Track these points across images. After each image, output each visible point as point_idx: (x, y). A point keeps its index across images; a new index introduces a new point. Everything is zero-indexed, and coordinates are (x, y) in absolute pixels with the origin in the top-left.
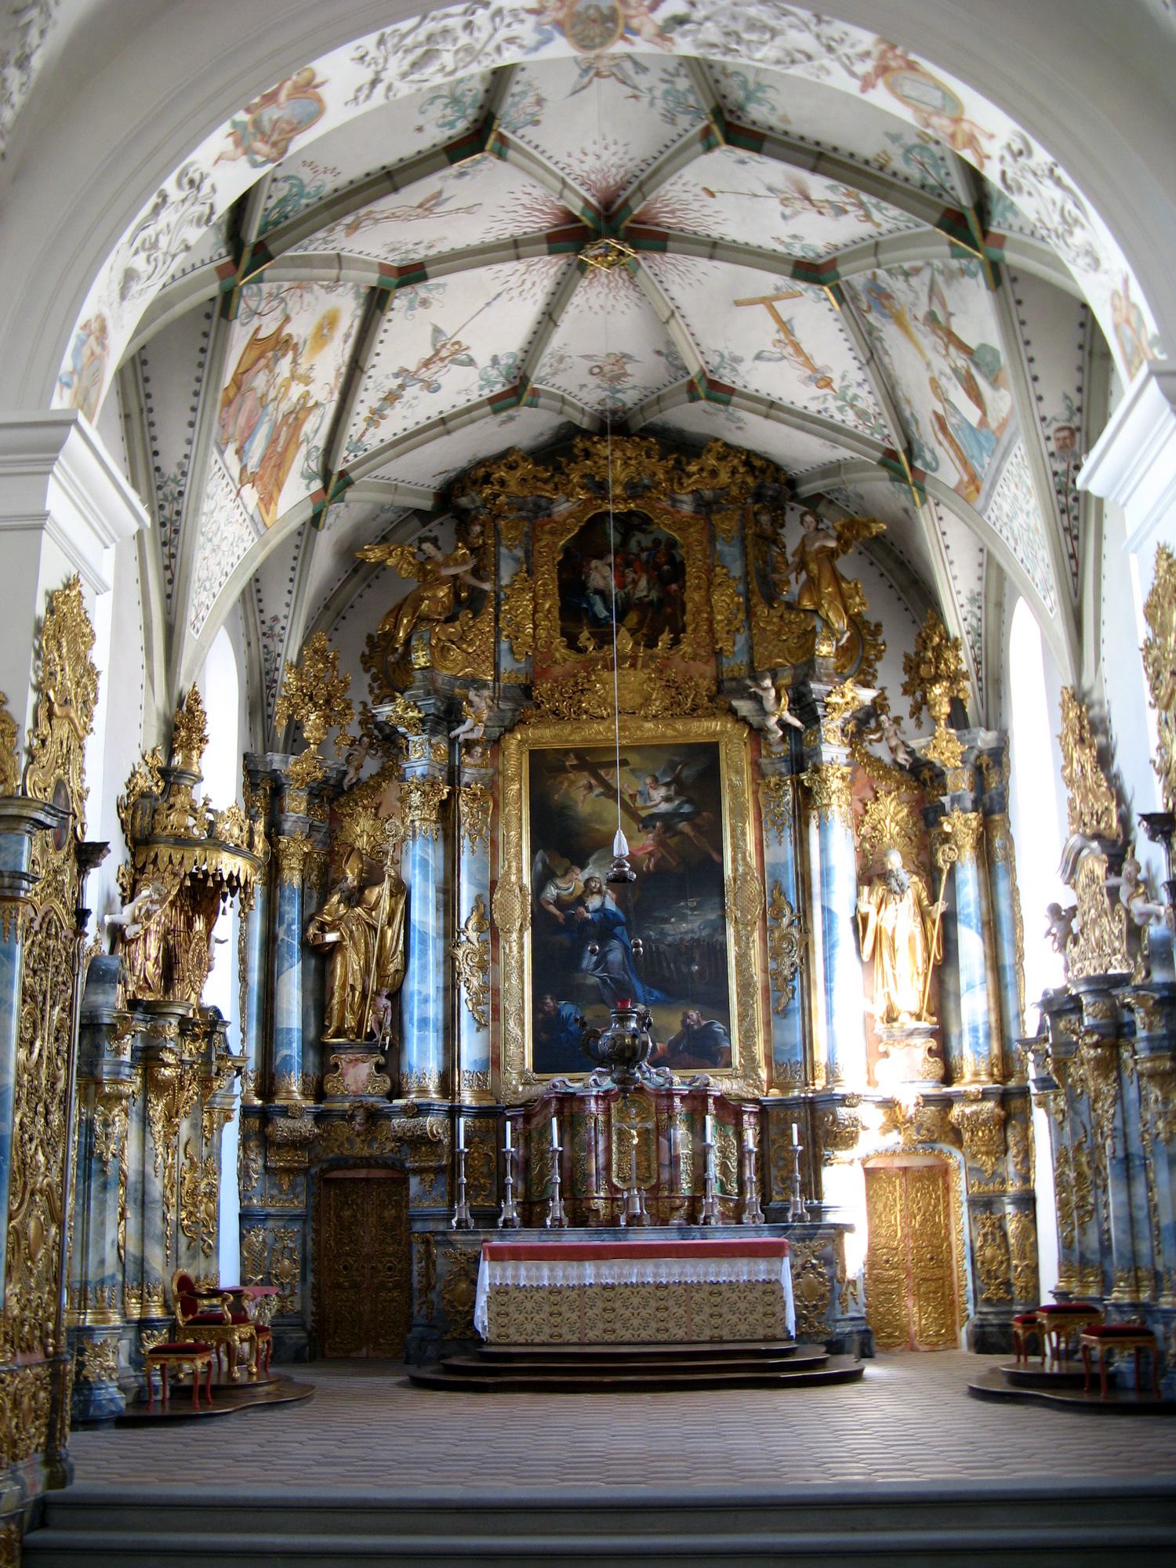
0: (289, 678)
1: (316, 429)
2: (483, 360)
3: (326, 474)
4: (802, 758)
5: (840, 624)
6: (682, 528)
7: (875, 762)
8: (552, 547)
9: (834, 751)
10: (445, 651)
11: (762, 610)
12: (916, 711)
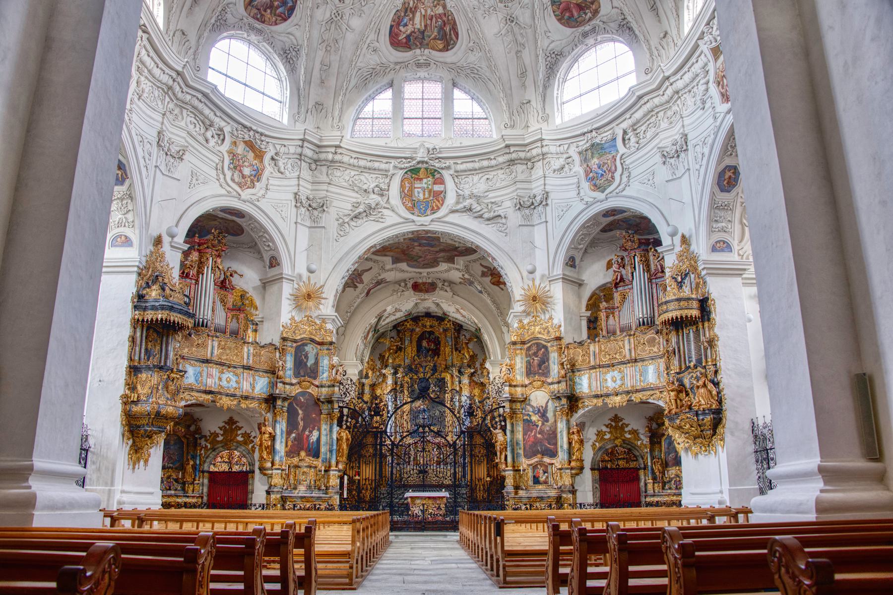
6: (440, 334)
7: (474, 381)
8: (415, 338)
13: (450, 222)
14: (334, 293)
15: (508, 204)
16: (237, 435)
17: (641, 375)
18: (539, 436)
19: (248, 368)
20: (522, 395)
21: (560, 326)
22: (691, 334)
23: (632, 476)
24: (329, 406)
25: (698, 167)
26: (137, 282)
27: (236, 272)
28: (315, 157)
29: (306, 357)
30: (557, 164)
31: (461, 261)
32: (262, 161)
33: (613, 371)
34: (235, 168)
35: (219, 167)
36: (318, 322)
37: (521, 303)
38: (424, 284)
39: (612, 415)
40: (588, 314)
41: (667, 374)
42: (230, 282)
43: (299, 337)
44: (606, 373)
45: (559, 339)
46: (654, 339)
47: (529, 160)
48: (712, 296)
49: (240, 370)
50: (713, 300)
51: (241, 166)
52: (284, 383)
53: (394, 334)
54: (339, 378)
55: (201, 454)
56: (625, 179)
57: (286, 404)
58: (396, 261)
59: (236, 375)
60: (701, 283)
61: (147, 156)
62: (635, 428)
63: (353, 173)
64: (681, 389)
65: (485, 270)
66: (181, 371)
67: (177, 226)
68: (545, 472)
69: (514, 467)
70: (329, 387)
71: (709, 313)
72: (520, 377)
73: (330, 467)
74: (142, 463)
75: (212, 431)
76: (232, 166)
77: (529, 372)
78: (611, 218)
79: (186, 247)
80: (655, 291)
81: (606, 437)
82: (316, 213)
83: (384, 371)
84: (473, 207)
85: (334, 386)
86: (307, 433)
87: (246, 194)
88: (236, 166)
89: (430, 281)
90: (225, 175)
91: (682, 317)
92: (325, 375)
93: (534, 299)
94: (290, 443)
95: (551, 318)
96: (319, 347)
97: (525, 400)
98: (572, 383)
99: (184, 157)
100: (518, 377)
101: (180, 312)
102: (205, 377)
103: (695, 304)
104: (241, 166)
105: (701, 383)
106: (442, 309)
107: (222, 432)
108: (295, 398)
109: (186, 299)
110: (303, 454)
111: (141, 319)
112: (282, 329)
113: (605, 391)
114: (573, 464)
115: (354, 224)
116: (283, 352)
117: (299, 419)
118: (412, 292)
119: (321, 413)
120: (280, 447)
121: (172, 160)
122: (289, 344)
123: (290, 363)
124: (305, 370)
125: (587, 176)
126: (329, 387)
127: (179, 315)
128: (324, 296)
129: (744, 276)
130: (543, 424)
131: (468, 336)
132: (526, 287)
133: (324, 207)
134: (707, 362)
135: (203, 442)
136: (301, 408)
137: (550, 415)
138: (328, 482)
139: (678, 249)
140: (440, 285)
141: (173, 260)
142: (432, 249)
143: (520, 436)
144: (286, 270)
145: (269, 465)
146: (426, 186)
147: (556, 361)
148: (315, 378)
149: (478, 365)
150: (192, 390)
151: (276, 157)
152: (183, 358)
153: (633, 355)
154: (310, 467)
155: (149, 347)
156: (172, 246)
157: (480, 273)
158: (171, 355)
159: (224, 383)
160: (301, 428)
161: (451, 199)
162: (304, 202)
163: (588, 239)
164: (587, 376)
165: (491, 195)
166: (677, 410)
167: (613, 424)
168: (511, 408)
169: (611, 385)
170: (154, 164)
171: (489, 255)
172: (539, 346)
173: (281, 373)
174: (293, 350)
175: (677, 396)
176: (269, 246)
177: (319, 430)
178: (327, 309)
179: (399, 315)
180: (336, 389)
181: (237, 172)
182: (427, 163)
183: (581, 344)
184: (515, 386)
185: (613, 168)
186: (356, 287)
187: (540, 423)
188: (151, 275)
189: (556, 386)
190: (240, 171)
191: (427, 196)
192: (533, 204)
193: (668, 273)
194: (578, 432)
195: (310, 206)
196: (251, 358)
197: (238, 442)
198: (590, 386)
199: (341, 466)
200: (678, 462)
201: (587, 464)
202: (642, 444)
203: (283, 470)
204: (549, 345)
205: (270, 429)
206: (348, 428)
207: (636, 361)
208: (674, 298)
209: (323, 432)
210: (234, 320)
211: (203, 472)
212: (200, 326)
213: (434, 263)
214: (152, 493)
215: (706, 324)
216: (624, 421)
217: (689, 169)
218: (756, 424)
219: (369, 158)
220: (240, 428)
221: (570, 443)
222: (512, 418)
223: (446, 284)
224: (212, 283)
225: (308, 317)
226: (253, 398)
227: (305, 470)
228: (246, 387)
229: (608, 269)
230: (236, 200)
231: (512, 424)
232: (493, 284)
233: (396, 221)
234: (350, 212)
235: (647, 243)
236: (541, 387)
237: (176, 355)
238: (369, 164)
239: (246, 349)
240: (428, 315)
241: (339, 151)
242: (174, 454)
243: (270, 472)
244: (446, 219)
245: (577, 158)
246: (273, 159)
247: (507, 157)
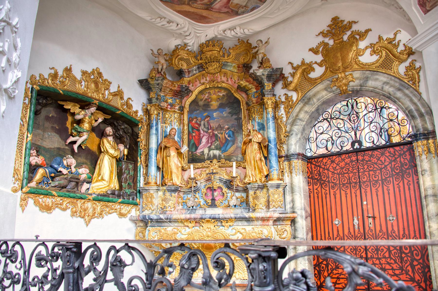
16: (359, 53)
75: (297, 62)
107: (319, 58)
197: (364, 67)
211: (288, 158)
220: (363, 35)
242: (220, 128)
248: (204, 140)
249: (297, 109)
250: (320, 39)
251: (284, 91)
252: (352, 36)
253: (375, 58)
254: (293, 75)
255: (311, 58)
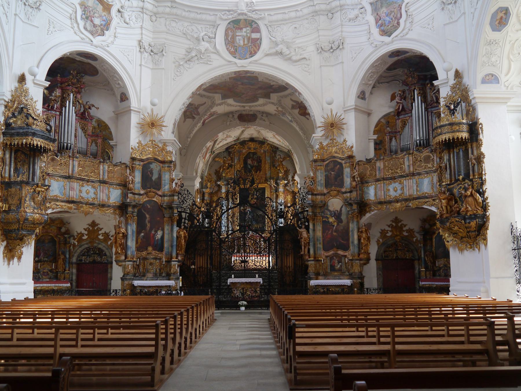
0: (205, 178)
1: (210, 148)
2: (233, 136)
3: (211, 152)
4: (277, 190)
5: (283, 172)
7: (288, 190)
8: (242, 157)
9: (281, 189)
10: (227, 173)
11: (272, 168)
12: (293, 184)
13: (264, 64)
14: (173, 122)
15: (312, 48)
17: (417, 186)
18: (335, 234)
19: (103, 182)
20: (322, 201)
21: (352, 147)
22: (461, 153)
23: (409, 265)
24: (170, 211)
25: (473, 10)
26: (4, 113)
27: (93, 106)
28: (155, 10)
29: (152, 173)
30: (352, 14)
31: (274, 97)
32: (109, 13)
33: (395, 182)
34: (87, 18)
35: (73, 17)
36: (160, 145)
37: (321, 129)
38: (247, 115)
39: (393, 217)
40: (375, 137)
41: (440, 185)
42: (89, 114)
43: (145, 158)
44: (389, 184)
45: (351, 157)
46: (429, 157)
47: (330, 11)
48: (480, 121)
49: (97, 185)
50: (481, 124)
51: (92, 17)
52: (134, 194)
53: (226, 154)
54: (178, 189)
55: (70, 250)
56: (408, 25)
57: (136, 210)
58: (225, 97)
59: (94, 187)
60: (471, 111)
61: (6, 5)
62: (411, 228)
63: (186, 24)
64: (452, 198)
65: (294, 104)
66: (46, 186)
67: (38, 66)
68: (339, 262)
69: (315, 258)
70: (170, 196)
71: (478, 134)
72: (321, 188)
73: (172, 258)
74: (16, 259)
75: (79, 232)
76: (84, 16)
77: (328, 184)
78: (396, 59)
79: (47, 84)
80: (430, 118)
81: (388, 235)
82: (156, 57)
83: (219, 183)
84: (283, 51)
85: (173, 196)
86: (153, 232)
87: (97, 40)
88: (88, 17)
89: (251, 113)
90: (78, 24)
91: (453, 138)
92: (167, 187)
93: (332, 125)
94: (139, 241)
95: (345, 140)
96: (161, 165)
97: (324, 205)
98: (363, 193)
99: (41, 7)
100: (319, 188)
101: (42, 137)
102: (68, 190)
103: (465, 128)
104: (92, 17)
105: (469, 193)
106: (262, 135)
107: (86, 233)
108: (143, 205)
109: (48, 127)
110: (150, 249)
111: (9, 143)
112: (131, 150)
113: (388, 199)
114: (362, 256)
115: (188, 66)
116: (132, 169)
117: (147, 221)
118: (238, 122)
119: (164, 217)
120: (131, 243)
121: (30, 10)
122: (137, 163)
123: (138, 177)
124: (150, 183)
125: (377, 23)
126: (170, 196)
127: (41, 140)
128: (164, 124)
129: (509, 104)
130: (338, 225)
131: (282, 156)
132: (326, 116)
133: (164, 53)
134: (474, 175)
135: (72, 241)
136: (148, 214)
137: (344, 217)
138: (170, 270)
139: (452, 81)
140: (259, 116)
141: (36, 95)
142: (251, 87)
143: (319, 234)
144: (134, 103)
145: (123, 258)
146: (245, 34)
147: (349, 175)
148: (159, 190)
149: (290, 178)
150: (58, 201)
151: (121, 10)
152: (48, 175)
153: (411, 169)
154: (156, 259)
155: (19, 166)
156: (35, 83)
157: (290, 106)
158: (38, 172)
159: (84, 195)
160: (148, 228)
161: (265, 45)
162: (147, 48)
163: (376, 76)
164: (373, 186)
165: (298, 41)
166: (447, 215)
167: (394, 224)
168: (313, 212)
169: (393, 194)
170: (14, 12)
171: (296, 90)
172: (336, 163)
173: (131, 186)
174: (141, 168)
175: (448, 203)
176: (119, 84)
177: (163, 230)
178: (168, 134)
179: (229, 140)
180: (176, 198)
181: (89, 22)
182: (246, 15)
183: (369, 161)
184: (316, 195)
185: (399, 15)
186: (194, 118)
187: (335, 224)
188: (17, 107)
189: (348, 195)
190: (92, 21)
191: (246, 42)
192: (332, 48)
193: (442, 102)
194: (366, 231)
195: (152, 51)
196: (106, 174)
197: (99, 239)
198: (375, 195)
199: (180, 258)
200: (447, 255)
201: (373, 256)
202: (417, 240)
203: (134, 262)
204: (343, 162)
205: (123, 230)
206: (185, 228)
207: (413, 175)
208: (447, 123)
209: (166, 231)
210: (94, 144)
211: (72, 263)
212: (62, 149)
213: (254, 99)
214: (24, 284)
215: (474, 145)
216: (402, 222)
217: (464, 13)
218: (514, 227)
219: (199, 11)
220: (101, 229)
221: (359, 240)
222: (314, 220)
223: (264, 115)
224: (74, 115)
225: (152, 141)
226: (109, 206)
227: (152, 261)
228: (102, 197)
229: (391, 101)
230: (89, 45)
231: (314, 225)
232: (301, 115)
233: (222, 64)
234: (184, 57)
235: (425, 78)
236: (337, 195)
237: (42, 172)
238: (199, 17)
239: (101, 167)
240: (252, 140)
241: (174, 5)
243: (124, 263)
244: (262, 61)
245: (369, 8)
246: (119, 11)
247: (311, 9)
248: (42, 255)
249: (77, 248)
250: (88, 226)
251: (73, 241)
252: (97, 229)
253: (102, 238)
254: (77, 236)
255: (84, 232)
